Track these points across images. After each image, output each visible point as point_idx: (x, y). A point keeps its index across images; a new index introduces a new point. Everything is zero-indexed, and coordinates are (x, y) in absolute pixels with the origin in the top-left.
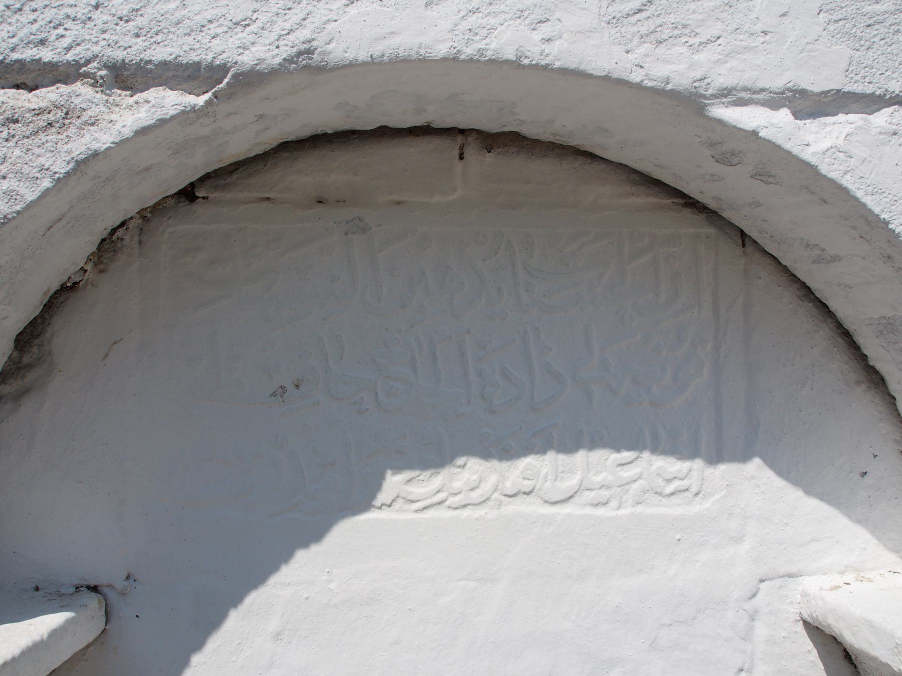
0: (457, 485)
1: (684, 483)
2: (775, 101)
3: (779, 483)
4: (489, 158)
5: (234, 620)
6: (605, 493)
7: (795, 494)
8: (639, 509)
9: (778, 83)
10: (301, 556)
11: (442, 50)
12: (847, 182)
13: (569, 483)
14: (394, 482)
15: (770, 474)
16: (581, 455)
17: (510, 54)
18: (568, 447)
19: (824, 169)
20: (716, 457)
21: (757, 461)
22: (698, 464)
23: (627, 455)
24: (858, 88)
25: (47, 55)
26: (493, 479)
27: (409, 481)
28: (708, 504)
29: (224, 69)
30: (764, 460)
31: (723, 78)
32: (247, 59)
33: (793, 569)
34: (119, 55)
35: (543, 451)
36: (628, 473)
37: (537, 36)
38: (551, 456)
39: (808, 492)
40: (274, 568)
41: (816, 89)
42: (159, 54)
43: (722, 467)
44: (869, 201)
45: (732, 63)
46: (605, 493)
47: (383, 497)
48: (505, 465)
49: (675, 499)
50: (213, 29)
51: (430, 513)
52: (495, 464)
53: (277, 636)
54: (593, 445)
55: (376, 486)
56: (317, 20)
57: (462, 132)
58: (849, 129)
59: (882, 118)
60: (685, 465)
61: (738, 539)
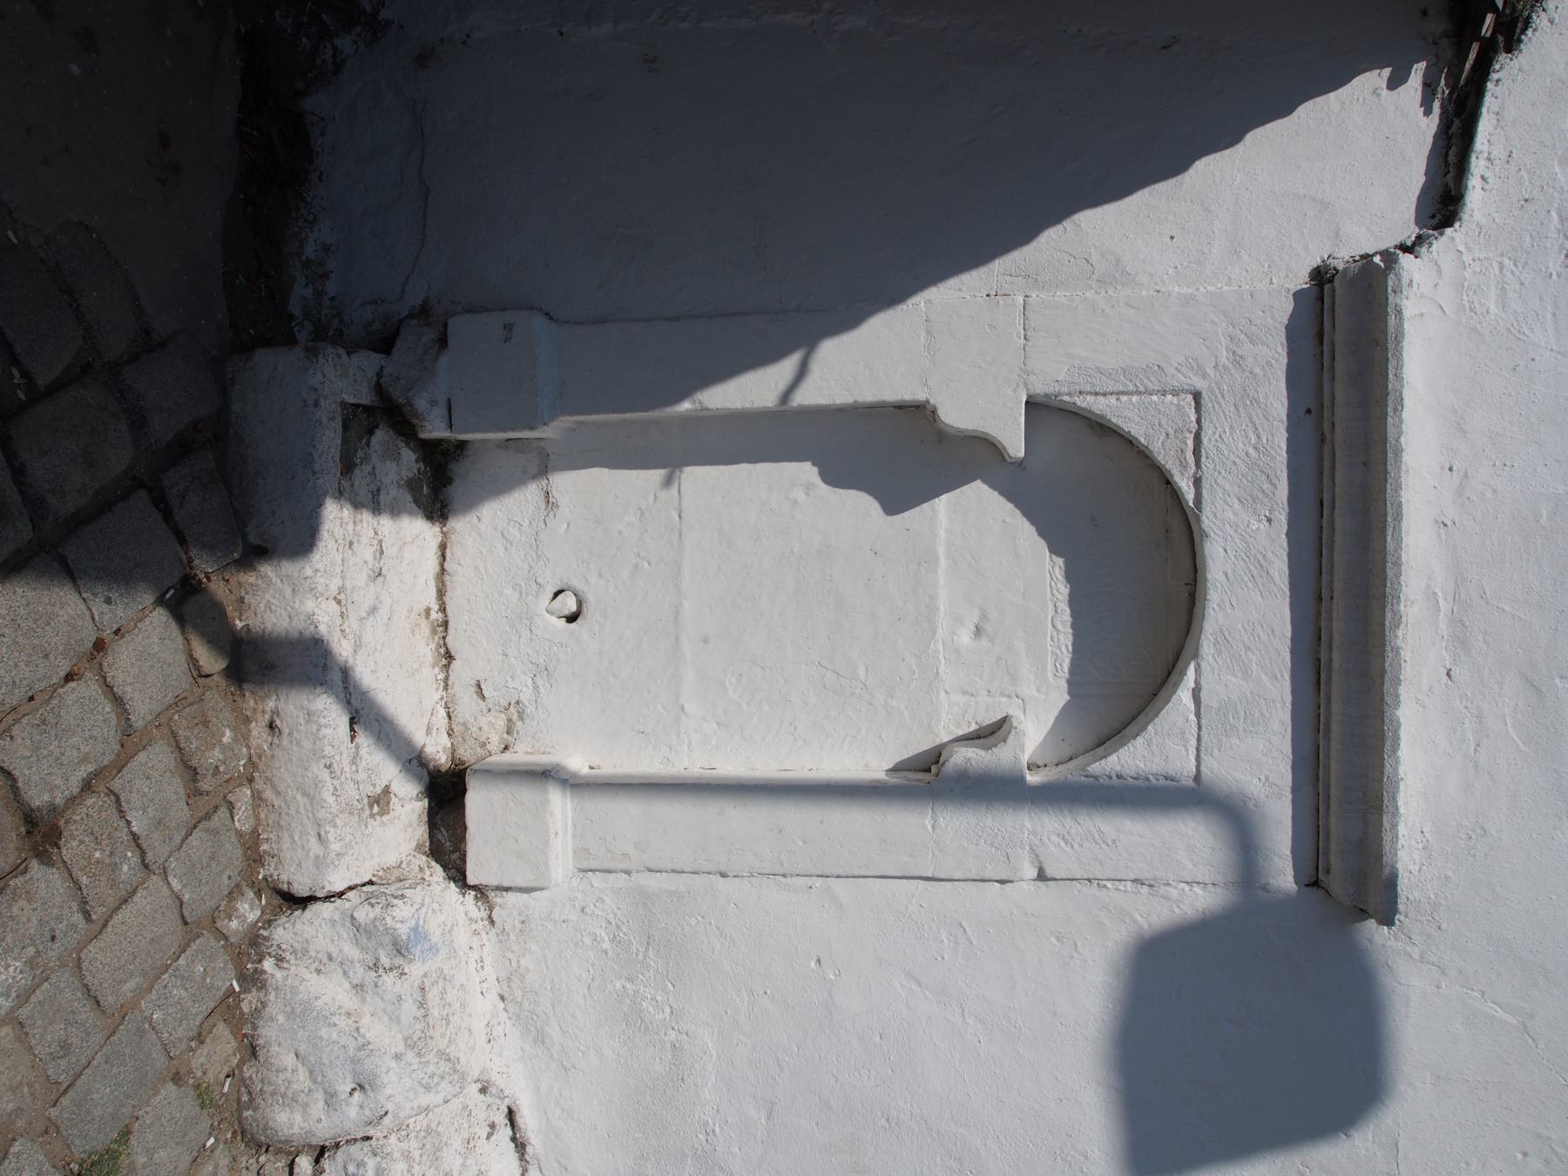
0: (1059, 585)
1: (1059, 670)
2: (1197, 682)
3: (1060, 707)
4: (1186, 595)
5: (1010, 506)
6: (1056, 640)
7: (1056, 712)
8: (1050, 653)
9: (1203, 683)
10: (1033, 529)
11: (1209, 576)
12: (1171, 704)
13: (1060, 627)
14: (1060, 561)
15: (1064, 703)
16: (1071, 631)
17: (1208, 597)
18: (1074, 626)
19: (1174, 696)
20: (1069, 682)
21: (1068, 698)
22: (1067, 676)
23: (1070, 648)
24: (1202, 709)
25: (1203, 459)
26: (1061, 598)
27: (1060, 567)
28: (1052, 680)
29: (1200, 512)
30: (1069, 701)
31: (1204, 665)
32: (1204, 518)
33: (1027, 712)
34: (1204, 481)
35: (1072, 617)
36: (1064, 651)
37: (1215, 606)
38: (1070, 619)
39: (1057, 718)
40: (1029, 520)
41: (1201, 694)
42: (1205, 493)
43: (1066, 685)
44: (1164, 711)
45: (1209, 668)
46: (1056, 640)
47: (1054, 557)
48: (1067, 602)
49: (1054, 668)
50: (1213, 507)
51: (1048, 575)
52: (1067, 598)
53: (1004, 521)
54: (1074, 635)
55: (1058, 554)
56: (1217, 538)
57: (1196, 585)
58: (1188, 705)
59: (1192, 717)
60: (1066, 671)
61: (1038, 691)
